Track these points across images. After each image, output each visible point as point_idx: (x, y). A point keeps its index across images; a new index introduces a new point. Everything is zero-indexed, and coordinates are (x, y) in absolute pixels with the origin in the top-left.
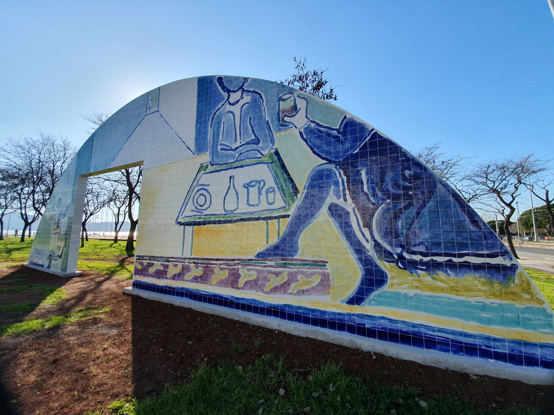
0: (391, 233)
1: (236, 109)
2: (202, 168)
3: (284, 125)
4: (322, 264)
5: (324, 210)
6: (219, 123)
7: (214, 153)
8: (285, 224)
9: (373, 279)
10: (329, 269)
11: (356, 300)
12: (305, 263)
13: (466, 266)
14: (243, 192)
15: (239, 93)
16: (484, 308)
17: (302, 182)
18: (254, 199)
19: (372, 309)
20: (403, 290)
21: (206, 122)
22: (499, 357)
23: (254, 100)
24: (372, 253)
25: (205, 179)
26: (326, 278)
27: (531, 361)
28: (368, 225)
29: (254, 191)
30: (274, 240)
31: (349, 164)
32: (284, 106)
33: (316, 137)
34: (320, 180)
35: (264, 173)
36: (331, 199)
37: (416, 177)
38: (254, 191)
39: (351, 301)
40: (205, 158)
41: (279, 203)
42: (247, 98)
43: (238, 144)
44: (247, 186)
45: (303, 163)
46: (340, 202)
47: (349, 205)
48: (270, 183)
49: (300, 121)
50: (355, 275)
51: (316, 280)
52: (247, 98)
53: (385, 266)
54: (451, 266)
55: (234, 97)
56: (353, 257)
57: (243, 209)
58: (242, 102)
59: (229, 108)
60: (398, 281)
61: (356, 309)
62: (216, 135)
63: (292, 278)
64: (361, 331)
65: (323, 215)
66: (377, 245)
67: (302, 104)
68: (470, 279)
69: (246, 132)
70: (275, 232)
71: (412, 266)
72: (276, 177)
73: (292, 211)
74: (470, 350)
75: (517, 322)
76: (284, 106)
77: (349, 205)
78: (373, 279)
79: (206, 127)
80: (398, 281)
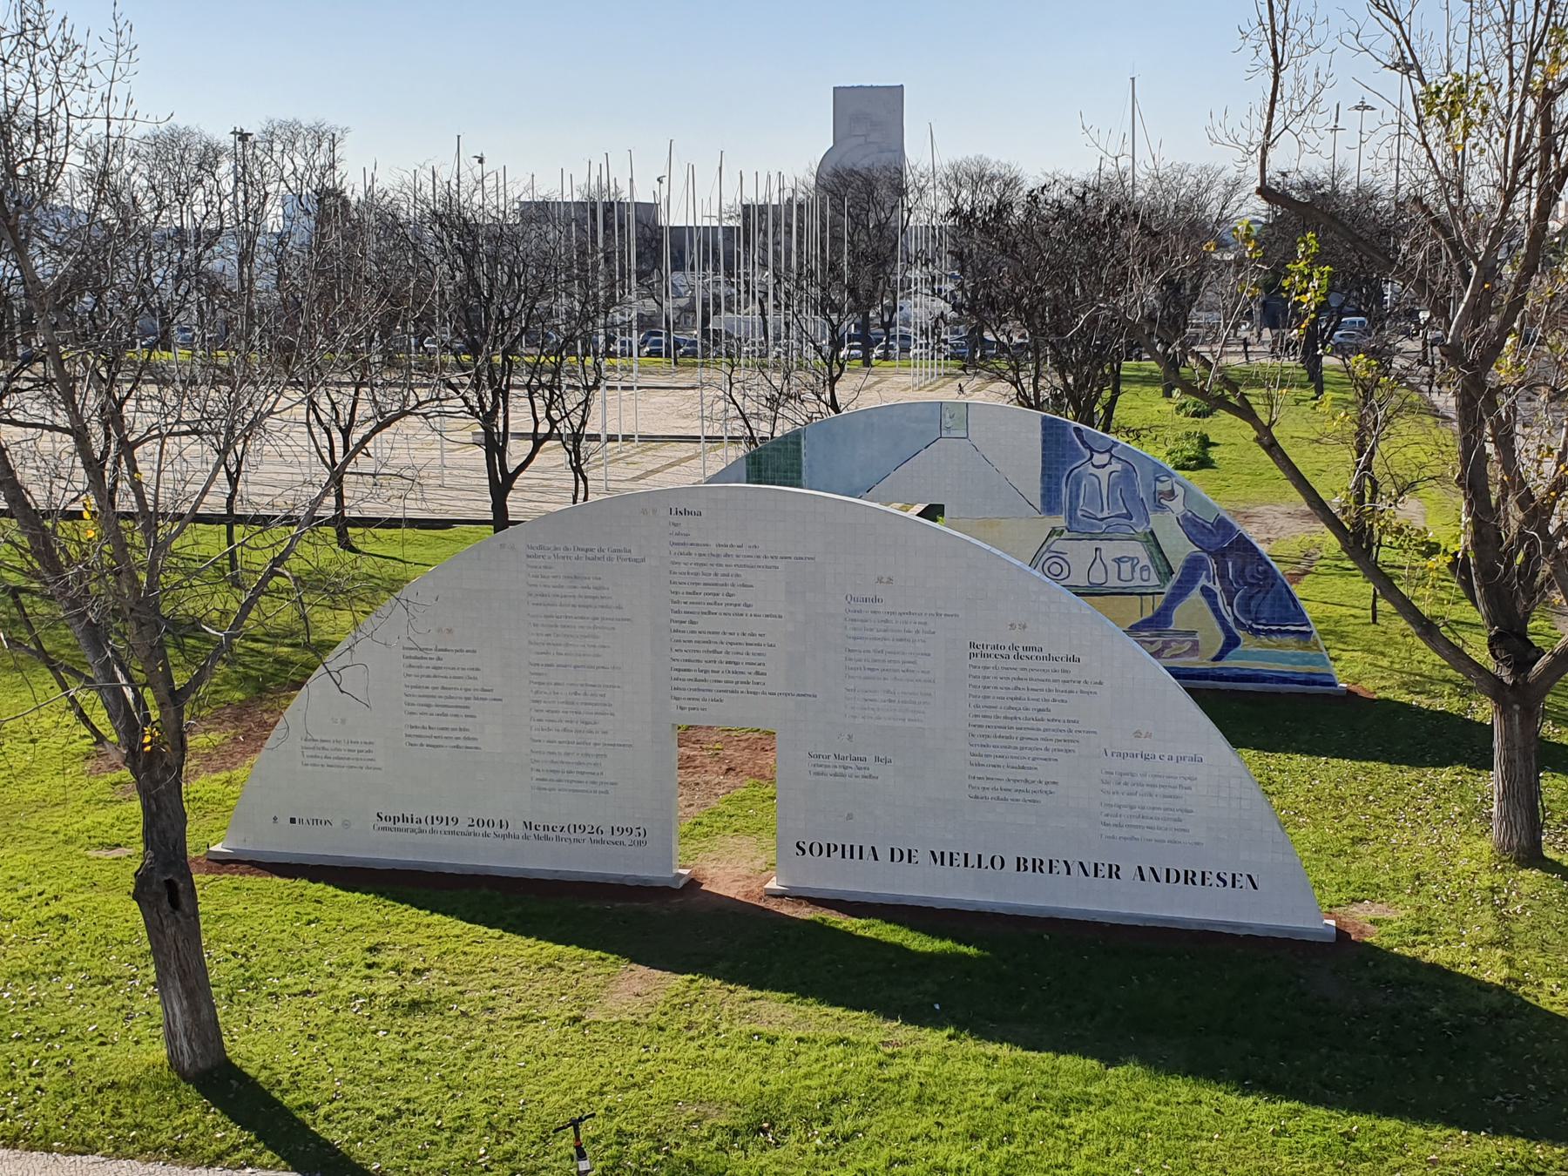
0: (1245, 609)
1: (1103, 474)
2: (1053, 532)
3: (1161, 507)
4: (1193, 633)
5: (1196, 591)
6: (1079, 485)
7: (1071, 517)
8: (1159, 601)
9: (1232, 642)
10: (1198, 637)
11: (1217, 658)
12: (1177, 633)
13: (1288, 632)
14: (1112, 567)
15: (1106, 457)
16: (1295, 656)
17: (1177, 565)
18: (1126, 574)
19: (1231, 663)
20: (1252, 649)
21: (1059, 478)
22: (1299, 683)
23: (1125, 471)
24: (1232, 625)
25: (1058, 545)
26: (1196, 643)
27: (1314, 683)
28: (1231, 605)
29: (1126, 567)
30: (1148, 614)
31: (1220, 555)
32: (1160, 486)
33: (1192, 526)
34: (1193, 568)
35: (1138, 550)
36: (1203, 581)
37: (1265, 572)
38: (1126, 567)
39: (1215, 659)
40: (1060, 521)
41: (1155, 580)
42: (1116, 466)
43: (1105, 514)
44: (1118, 561)
45: (1179, 548)
46: (1210, 585)
47: (1217, 588)
48: (1145, 561)
49: (1177, 506)
50: (1220, 639)
51: (1187, 646)
52: (1116, 466)
53: (1240, 633)
54: (1280, 632)
55: (1100, 459)
56: (1218, 628)
57: (1113, 582)
58: (1109, 468)
59: (1093, 470)
60: (1247, 643)
61: (1219, 664)
62: (1075, 497)
63: (1166, 645)
64: (1221, 678)
65: (1195, 594)
66: (1236, 619)
67: (1179, 490)
68: (1289, 639)
69: (1116, 502)
70: (1150, 607)
71: (1257, 632)
72: (1151, 558)
73: (1167, 589)
74: (1285, 680)
75: (1308, 663)
76: (1160, 486)
77: (1217, 588)
78: (1232, 642)
79: (1058, 484)
80: (1247, 643)
